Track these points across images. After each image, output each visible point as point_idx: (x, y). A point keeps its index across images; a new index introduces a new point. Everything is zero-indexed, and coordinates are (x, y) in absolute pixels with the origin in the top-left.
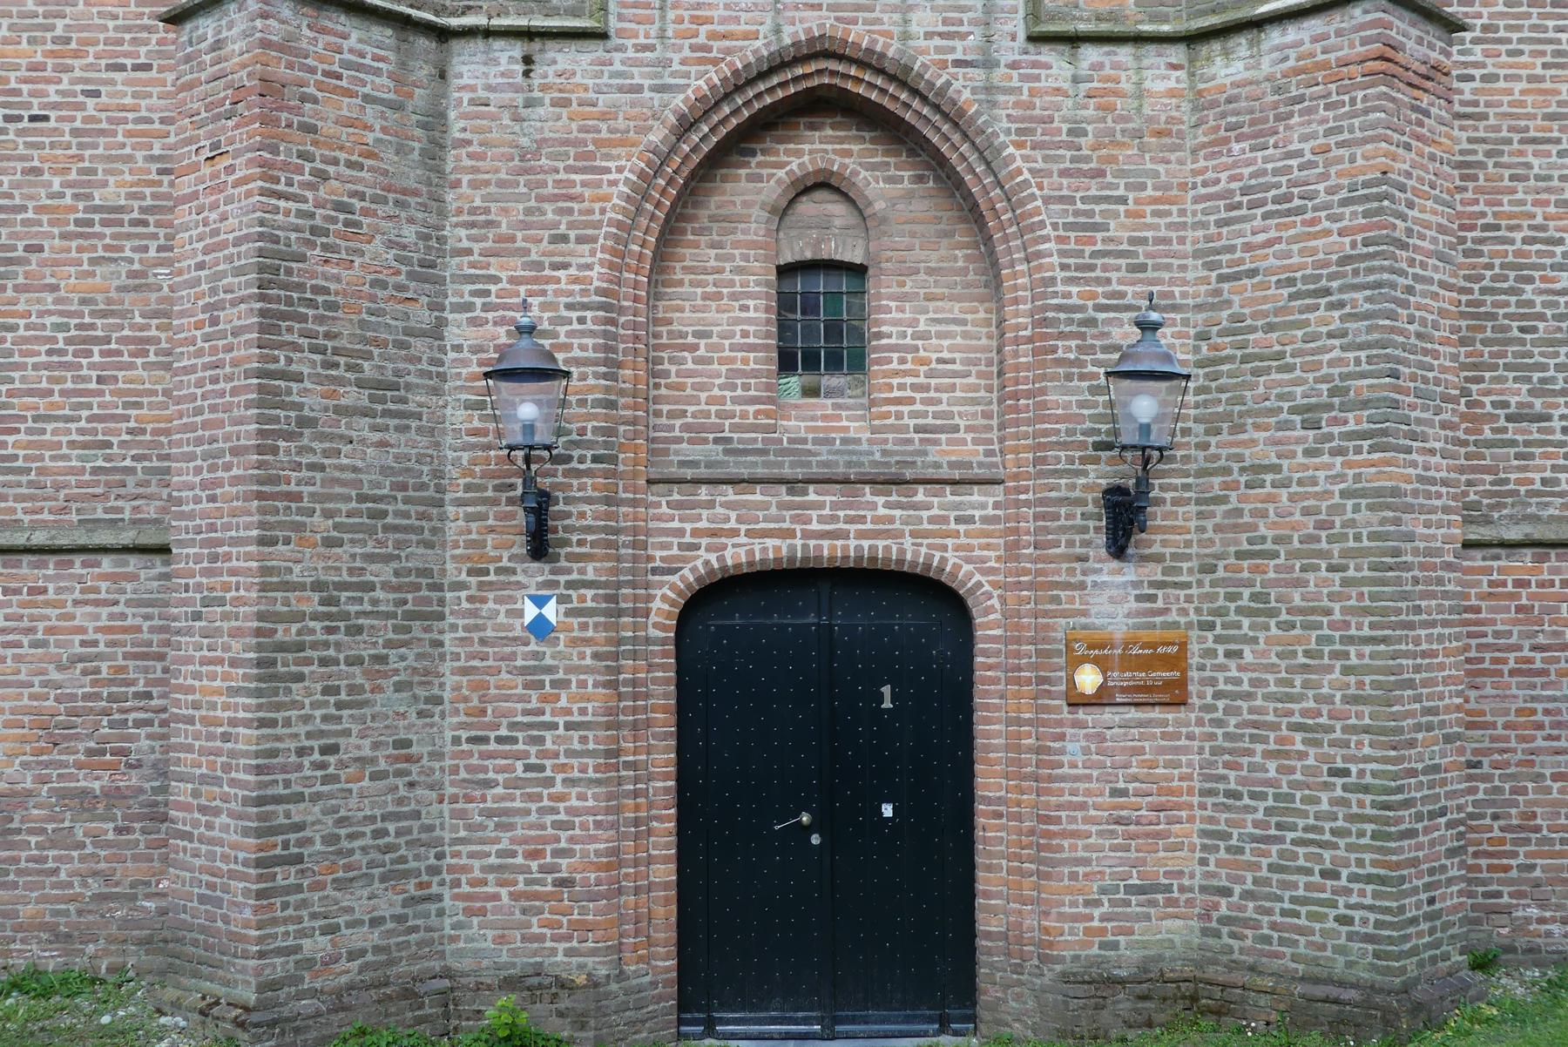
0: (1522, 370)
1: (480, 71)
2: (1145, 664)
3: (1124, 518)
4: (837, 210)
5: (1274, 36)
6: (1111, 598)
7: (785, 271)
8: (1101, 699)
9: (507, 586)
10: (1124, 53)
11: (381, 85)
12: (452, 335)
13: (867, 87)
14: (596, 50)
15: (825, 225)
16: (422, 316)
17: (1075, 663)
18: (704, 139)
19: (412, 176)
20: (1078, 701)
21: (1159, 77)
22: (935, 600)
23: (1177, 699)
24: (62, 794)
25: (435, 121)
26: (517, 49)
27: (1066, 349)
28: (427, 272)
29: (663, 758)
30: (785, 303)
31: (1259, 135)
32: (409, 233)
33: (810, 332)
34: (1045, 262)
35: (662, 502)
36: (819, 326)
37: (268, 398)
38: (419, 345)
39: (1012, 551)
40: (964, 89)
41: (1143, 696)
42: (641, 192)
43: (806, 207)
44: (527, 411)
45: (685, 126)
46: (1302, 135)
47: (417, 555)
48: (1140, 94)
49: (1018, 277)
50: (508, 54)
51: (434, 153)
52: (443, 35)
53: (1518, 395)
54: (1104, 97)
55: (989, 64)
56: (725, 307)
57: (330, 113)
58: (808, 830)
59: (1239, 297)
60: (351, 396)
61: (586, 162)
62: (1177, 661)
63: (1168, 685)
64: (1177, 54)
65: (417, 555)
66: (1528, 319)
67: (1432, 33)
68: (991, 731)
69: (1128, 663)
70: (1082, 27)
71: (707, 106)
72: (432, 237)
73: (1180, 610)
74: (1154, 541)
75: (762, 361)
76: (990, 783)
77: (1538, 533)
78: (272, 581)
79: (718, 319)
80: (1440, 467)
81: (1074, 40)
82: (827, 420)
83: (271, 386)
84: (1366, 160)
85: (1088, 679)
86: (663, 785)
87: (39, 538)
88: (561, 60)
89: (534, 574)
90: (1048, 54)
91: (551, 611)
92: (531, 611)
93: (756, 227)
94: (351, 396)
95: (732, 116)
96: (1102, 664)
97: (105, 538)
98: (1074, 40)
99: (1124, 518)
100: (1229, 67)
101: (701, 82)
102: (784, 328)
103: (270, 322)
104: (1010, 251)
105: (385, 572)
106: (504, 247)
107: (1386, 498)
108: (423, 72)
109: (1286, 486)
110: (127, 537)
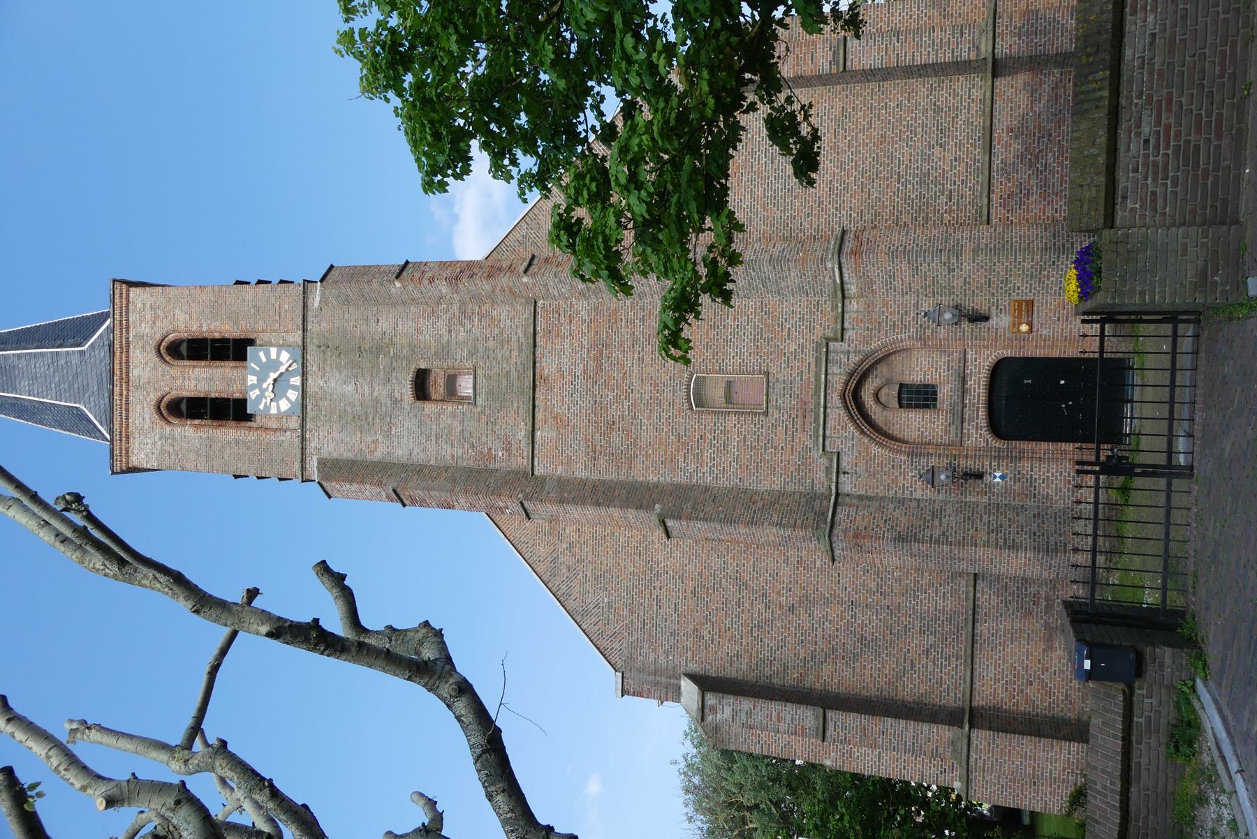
0: (936, 197)
1: (847, 487)
2: (1020, 311)
3: (979, 318)
4: (883, 391)
5: (846, 279)
6: (1001, 321)
7: (901, 406)
8: (1030, 324)
9: (991, 485)
10: (846, 316)
11: (852, 511)
12: (918, 495)
13: (853, 384)
14: (842, 455)
15: (888, 395)
16: (914, 504)
17: (1019, 331)
18: (866, 428)
19: (875, 504)
20: (1031, 331)
21: (853, 306)
22: (999, 369)
23: (1030, 303)
24: (1046, 613)
25: (860, 498)
26: (841, 476)
27: (929, 332)
28: (902, 502)
29: (1043, 446)
30: (909, 406)
31: (872, 282)
32: (891, 506)
33: (917, 399)
34: (903, 338)
35: (967, 443)
36: (920, 397)
37: (937, 542)
38: (922, 505)
39: (986, 347)
40: (855, 359)
41: (1030, 312)
42: (880, 444)
43: (882, 400)
44: (943, 477)
45: (863, 432)
46: (873, 272)
47: (981, 509)
48: (857, 312)
49: (907, 344)
50: (843, 478)
51: (870, 499)
52: (837, 494)
53: (944, 199)
54: (859, 321)
55: (849, 352)
56: (912, 423)
57: (861, 523)
58: (1067, 405)
59: (915, 287)
60: (936, 522)
61: (873, 459)
62: (1020, 303)
63: (1027, 306)
64: (847, 302)
65: (981, 509)
66: (921, 196)
67: (846, 237)
68: (1039, 353)
69: (1020, 316)
70: (839, 327)
71: (858, 427)
72: (892, 500)
73: (1005, 302)
74: (984, 309)
75: (927, 414)
76: (1055, 353)
77: (985, 193)
78: (987, 544)
79: (915, 425)
80: (966, 234)
81: (843, 329)
82: (946, 393)
83: (934, 541)
84: (882, 258)
85: (1024, 328)
86: (1051, 446)
87: (970, 612)
88: (844, 464)
89: (987, 478)
90: (846, 337)
91: (998, 474)
92: (998, 480)
93: (889, 414)
94: (936, 522)
95: (860, 420)
96: (1020, 324)
97: (971, 595)
98: (843, 329)
99: (979, 318)
100: (852, 289)
101: (851, 428)
102: (917, 406)
103: (917, 540)
104: (899, 346)
105: (985, 518)
106: (895, 482)
107: (975, 251)
108: (847, 500)
109: (969, 277)
110: (971, 589)
